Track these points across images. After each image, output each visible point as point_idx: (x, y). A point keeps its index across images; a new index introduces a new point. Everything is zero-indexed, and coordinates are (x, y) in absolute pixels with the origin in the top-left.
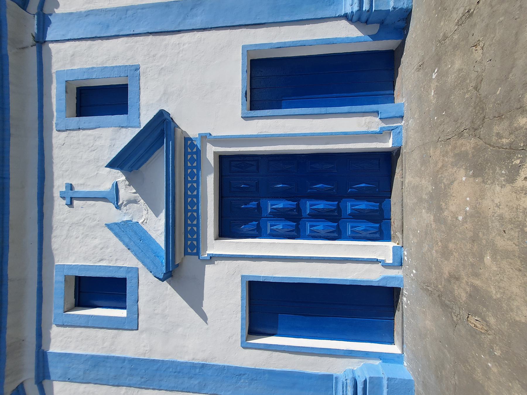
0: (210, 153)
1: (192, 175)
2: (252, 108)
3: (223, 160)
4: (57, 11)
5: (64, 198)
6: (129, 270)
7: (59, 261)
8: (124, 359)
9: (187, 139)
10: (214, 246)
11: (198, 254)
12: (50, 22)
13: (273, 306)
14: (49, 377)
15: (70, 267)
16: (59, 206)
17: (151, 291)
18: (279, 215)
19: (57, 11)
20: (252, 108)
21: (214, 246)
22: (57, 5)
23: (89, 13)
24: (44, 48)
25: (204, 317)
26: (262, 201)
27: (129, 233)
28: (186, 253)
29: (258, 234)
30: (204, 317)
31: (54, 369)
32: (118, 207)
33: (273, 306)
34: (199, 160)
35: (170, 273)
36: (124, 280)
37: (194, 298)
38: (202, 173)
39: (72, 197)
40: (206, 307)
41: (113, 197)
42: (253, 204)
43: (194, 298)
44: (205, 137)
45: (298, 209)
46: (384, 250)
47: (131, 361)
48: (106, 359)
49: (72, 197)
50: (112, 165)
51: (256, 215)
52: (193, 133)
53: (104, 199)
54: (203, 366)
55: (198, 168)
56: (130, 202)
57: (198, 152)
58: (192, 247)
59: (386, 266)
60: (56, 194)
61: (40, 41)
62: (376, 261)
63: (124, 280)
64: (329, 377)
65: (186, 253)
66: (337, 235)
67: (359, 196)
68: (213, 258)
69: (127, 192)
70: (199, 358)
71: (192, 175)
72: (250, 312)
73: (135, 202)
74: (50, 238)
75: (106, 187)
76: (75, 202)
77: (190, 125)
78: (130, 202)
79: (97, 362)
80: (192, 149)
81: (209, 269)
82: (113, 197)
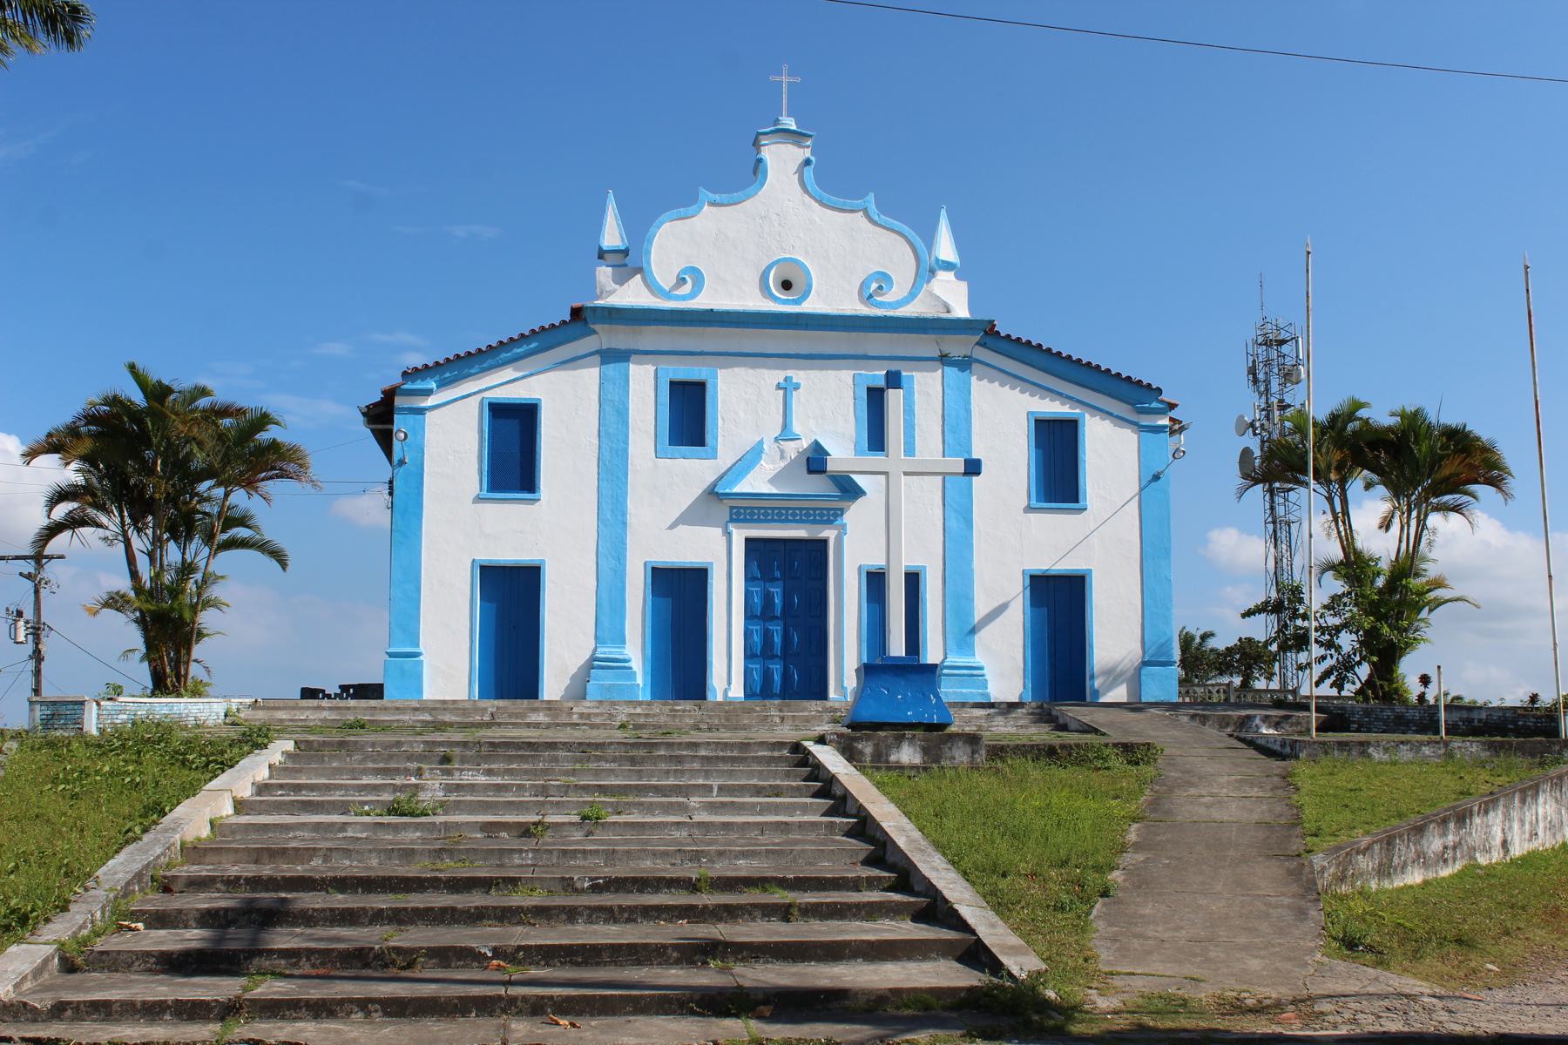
0: (829, 534)
1: (808, 515)
2: (868, 573)
3: (824, 542)
4: (974, 379)
5: (786, 379)
6: (715, 450)
7: (721, 373)
8: (626, 442)
9: (842, 511)
10: (739, 535)
11: (732, 520)
12: (963, 371)
13: (680, 592)
14: (603, 363)
15: (715, 386)
16: (779, 376)
17: (693, 473)
18: (768, 599)
19: (974, 379)
20: (868, 573)
21: (739, 535)
22: (980, 379)
23: (968, 411)
24: (938, 364)
25: (672, 527)
26: (781, 583)
27: (752, 457)
28: (732, 508)
29: (749, 578)
30: (672, 527)
31: (612, 369)
32: (776, 440)
33: (680, 592)
34: (822, 522)
35: (713, 493)
36: (702, 443)
37: (691, 517)
38: (808, 526)
39: (787, 388)
40: (681, 527)
41: (786, 434)
42: (778, 574)
43: (691, 517)
44: (844, 526)
45: (774, 618)
46: (737, 692)
47: (626, 450)
48: (626, 424)
49: (787, 388)
50: (816, 443)
51: (767, 577)
52: (848, 518)
53: (786, 425)
54: (625, 524)
55: (814, 522)
56: (782, 452)
57: (829, 522)
58: (738, 514)
59: (726, 691)
60: (789, 373)
61: (944, 359)
62: (729, 683)
63: (702, 443)
64: (624, 642)
65: (732, 508)
66: (749, 655)
67: (786, 676)
68: (728, 535)
69: (792, 449)
70: (631, 519)
71: (808, 515)
72: (672, 570)
73: (782, 457)
74: (745, 366)
75: (797, 428)
76: (781, 392)
77: (855, 514)
78: (782, 452)
79: (622, 414)
80: (831, 516)
81: (719, 531)
82: (786, 434)
